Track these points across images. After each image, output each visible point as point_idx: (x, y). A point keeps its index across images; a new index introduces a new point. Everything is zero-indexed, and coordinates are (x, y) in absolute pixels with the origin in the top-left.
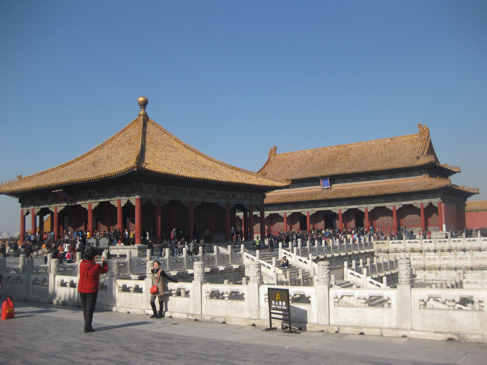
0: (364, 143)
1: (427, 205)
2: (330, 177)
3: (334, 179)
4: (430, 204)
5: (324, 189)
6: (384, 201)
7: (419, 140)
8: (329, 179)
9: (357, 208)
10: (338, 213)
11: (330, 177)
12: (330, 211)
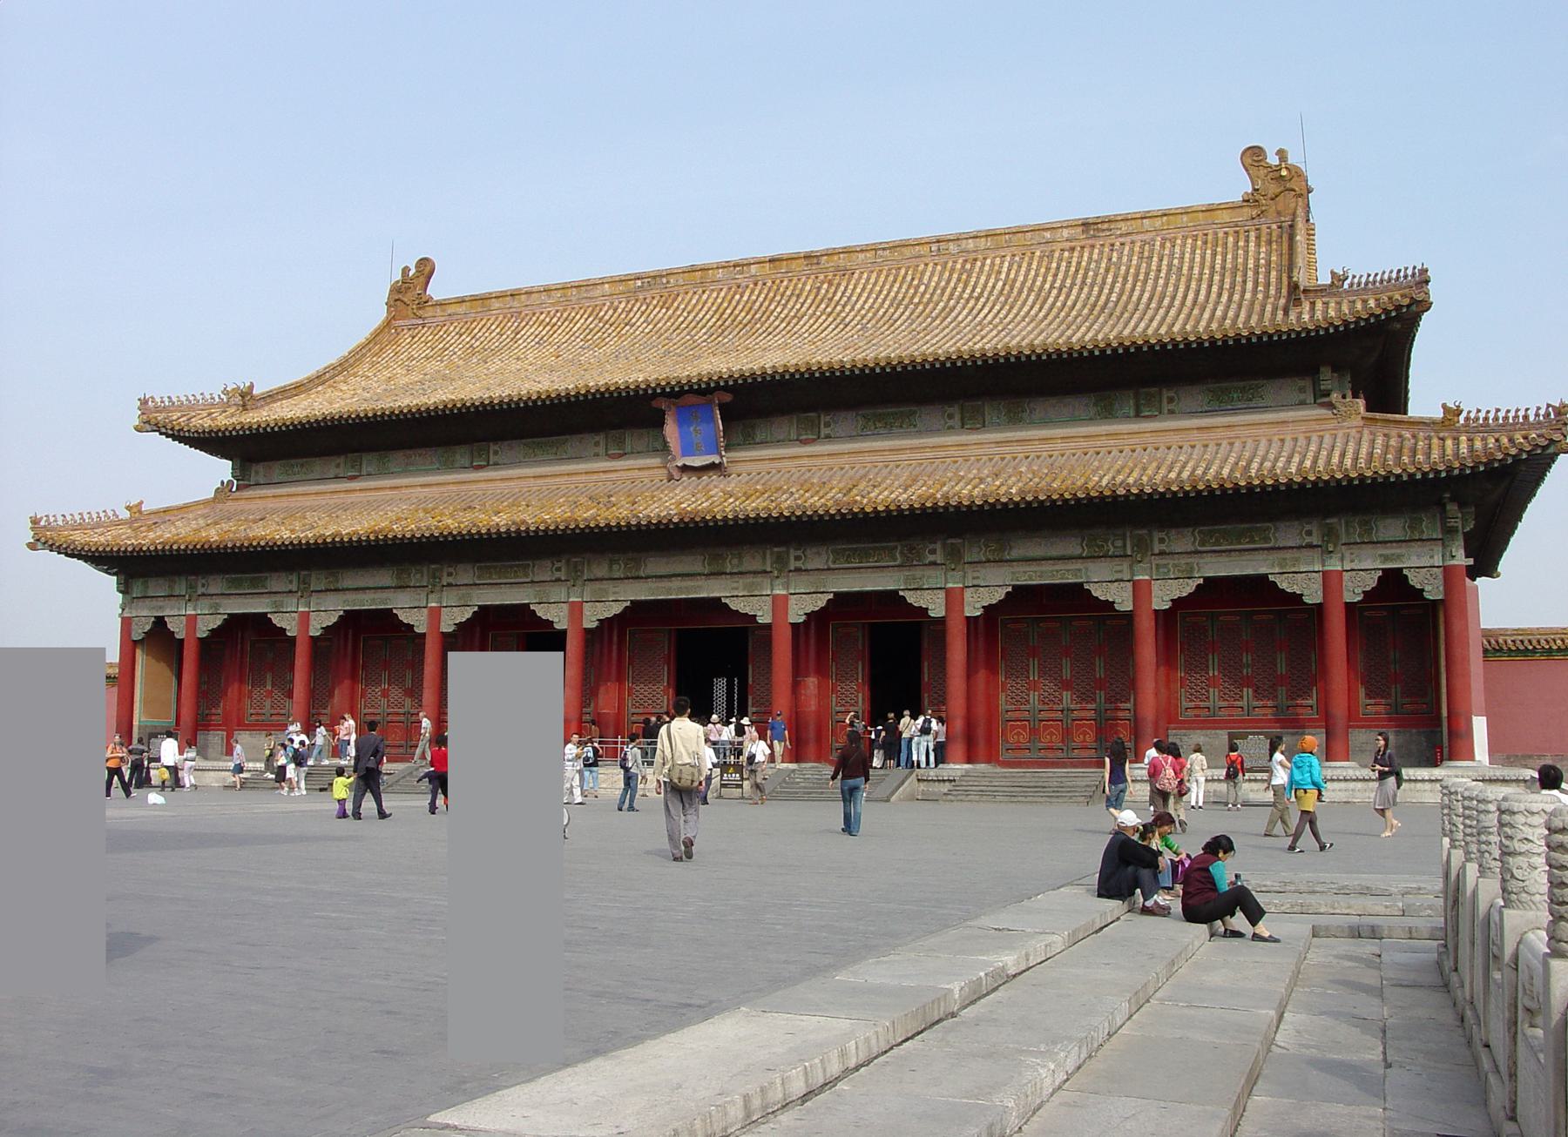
0: (926, 248)
1: (1371, 582)
2: (728, 398)
3: (758, 405)
4: (1393, 580)
5: (685, 469)
6: (1078, 551)
7: (1252, 234)
8: (722, 407)
9: (896, 592)
10: (764, 618)
11: (728, 398)
12: (715, 606)
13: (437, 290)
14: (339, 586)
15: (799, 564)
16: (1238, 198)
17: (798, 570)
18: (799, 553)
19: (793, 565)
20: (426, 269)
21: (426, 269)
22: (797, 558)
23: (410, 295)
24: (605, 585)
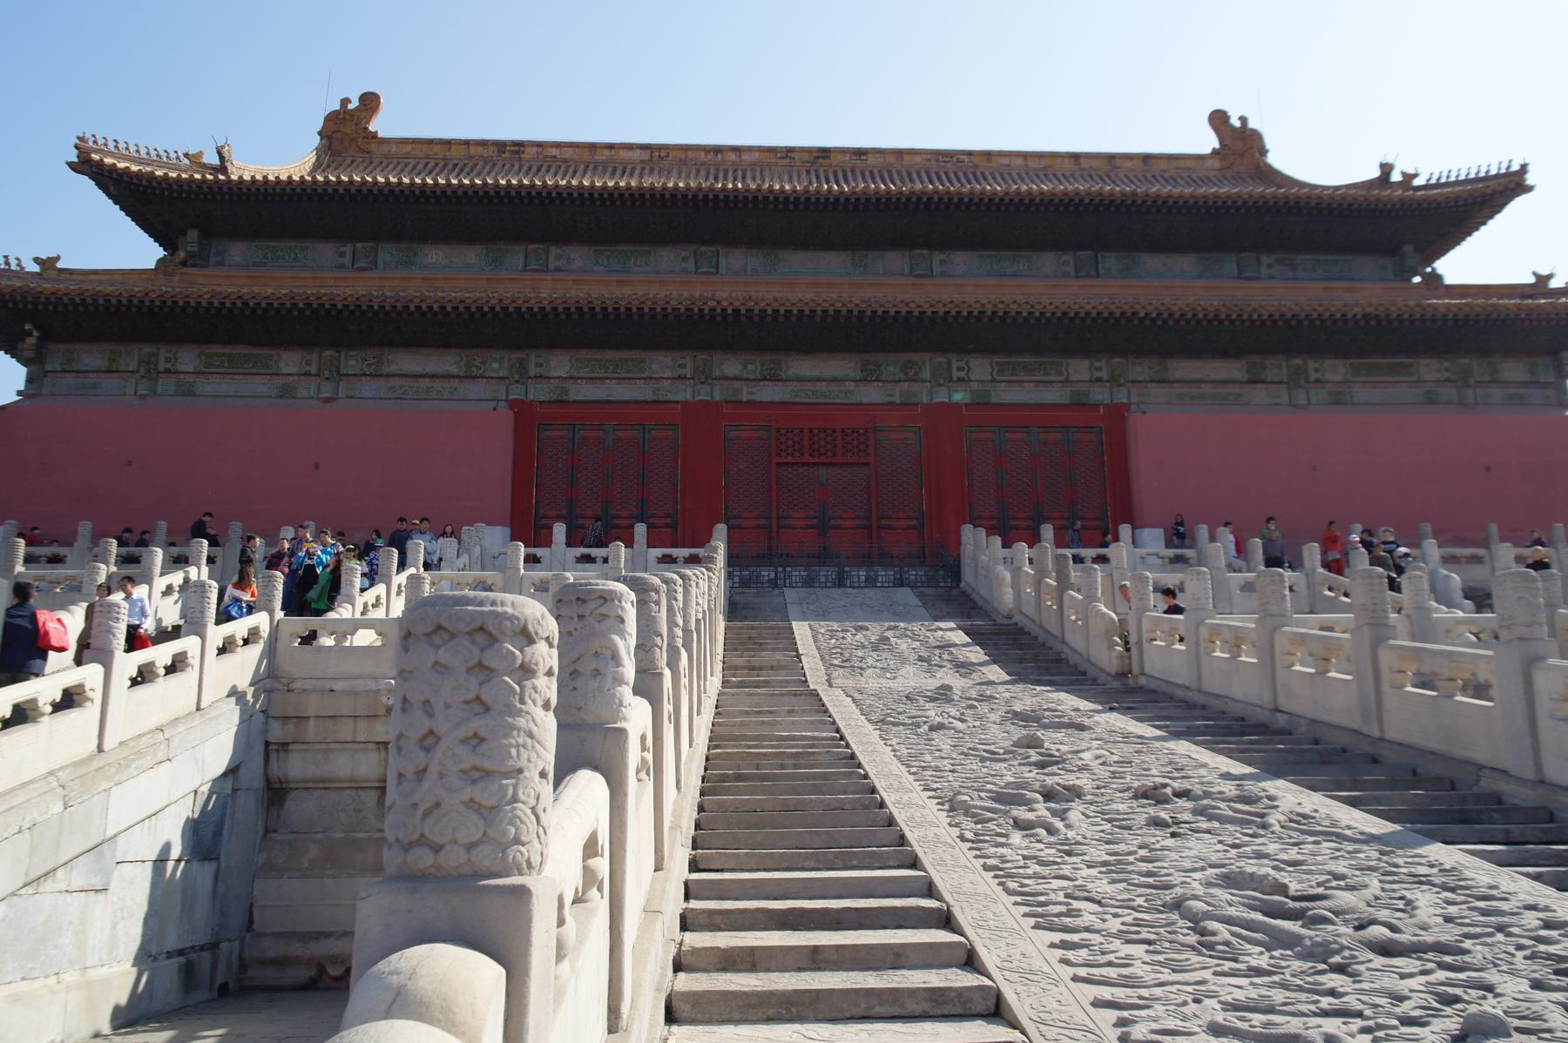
6: (1237, 375)
13: (383, 125)
14: (386, 370)
15: (962, 374)
16: (1208, 151)
17: (960, 380)
18: (962, 364)
19: (956, 375)
20: (370, 102)
21: (370, 102)
22: (960, 369)
23: (346, 129)
24: (736, 384)
